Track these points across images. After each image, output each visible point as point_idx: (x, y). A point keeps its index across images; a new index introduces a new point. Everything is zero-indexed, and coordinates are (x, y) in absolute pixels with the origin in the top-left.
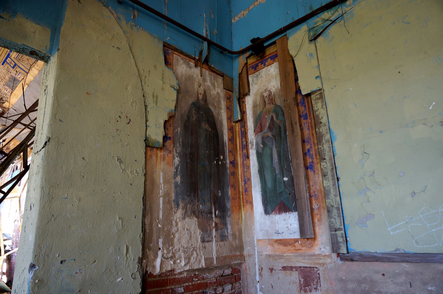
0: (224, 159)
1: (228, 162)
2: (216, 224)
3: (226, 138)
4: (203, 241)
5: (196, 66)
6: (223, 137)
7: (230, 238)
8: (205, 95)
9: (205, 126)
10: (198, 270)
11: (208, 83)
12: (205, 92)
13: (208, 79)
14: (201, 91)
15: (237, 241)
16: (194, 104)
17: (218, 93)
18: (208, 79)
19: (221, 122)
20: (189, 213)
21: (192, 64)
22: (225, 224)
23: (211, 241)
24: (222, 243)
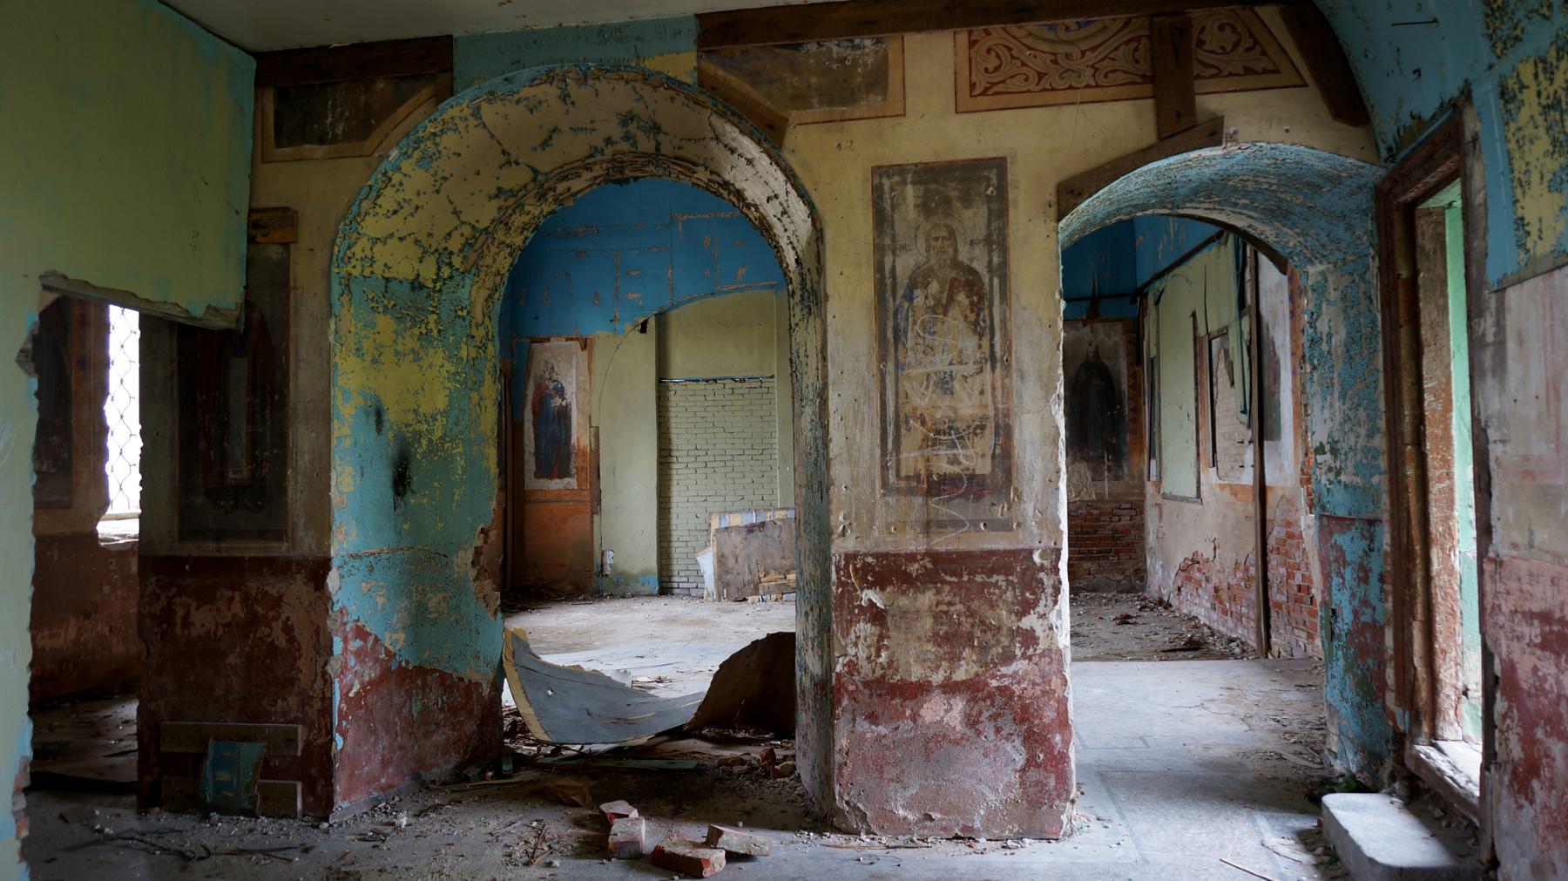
0: (1122, 407)
1: (1127, 409)
2: (1109, 467)
3: (1125, 387)
4: (1093, 480)
5: (1085, 325)
6: (1120, 386)
7: (1127, 478)
8: (1097, 352)
9: (1097, 382)
10: (1093, 501)
11: (1102, 336)
12: (1097, 347)
13: (1101, 332)
14: (1092, 349)
15: (1136, 481)
16: (1082, 365)
17: (1115, 342)
18: (1101, 332)
19: (1119, 373)
20: (1078, 458)
21: (1080, 325)
22: (1120, 467)
23: (1104, 480)
24: (1116, 482)
